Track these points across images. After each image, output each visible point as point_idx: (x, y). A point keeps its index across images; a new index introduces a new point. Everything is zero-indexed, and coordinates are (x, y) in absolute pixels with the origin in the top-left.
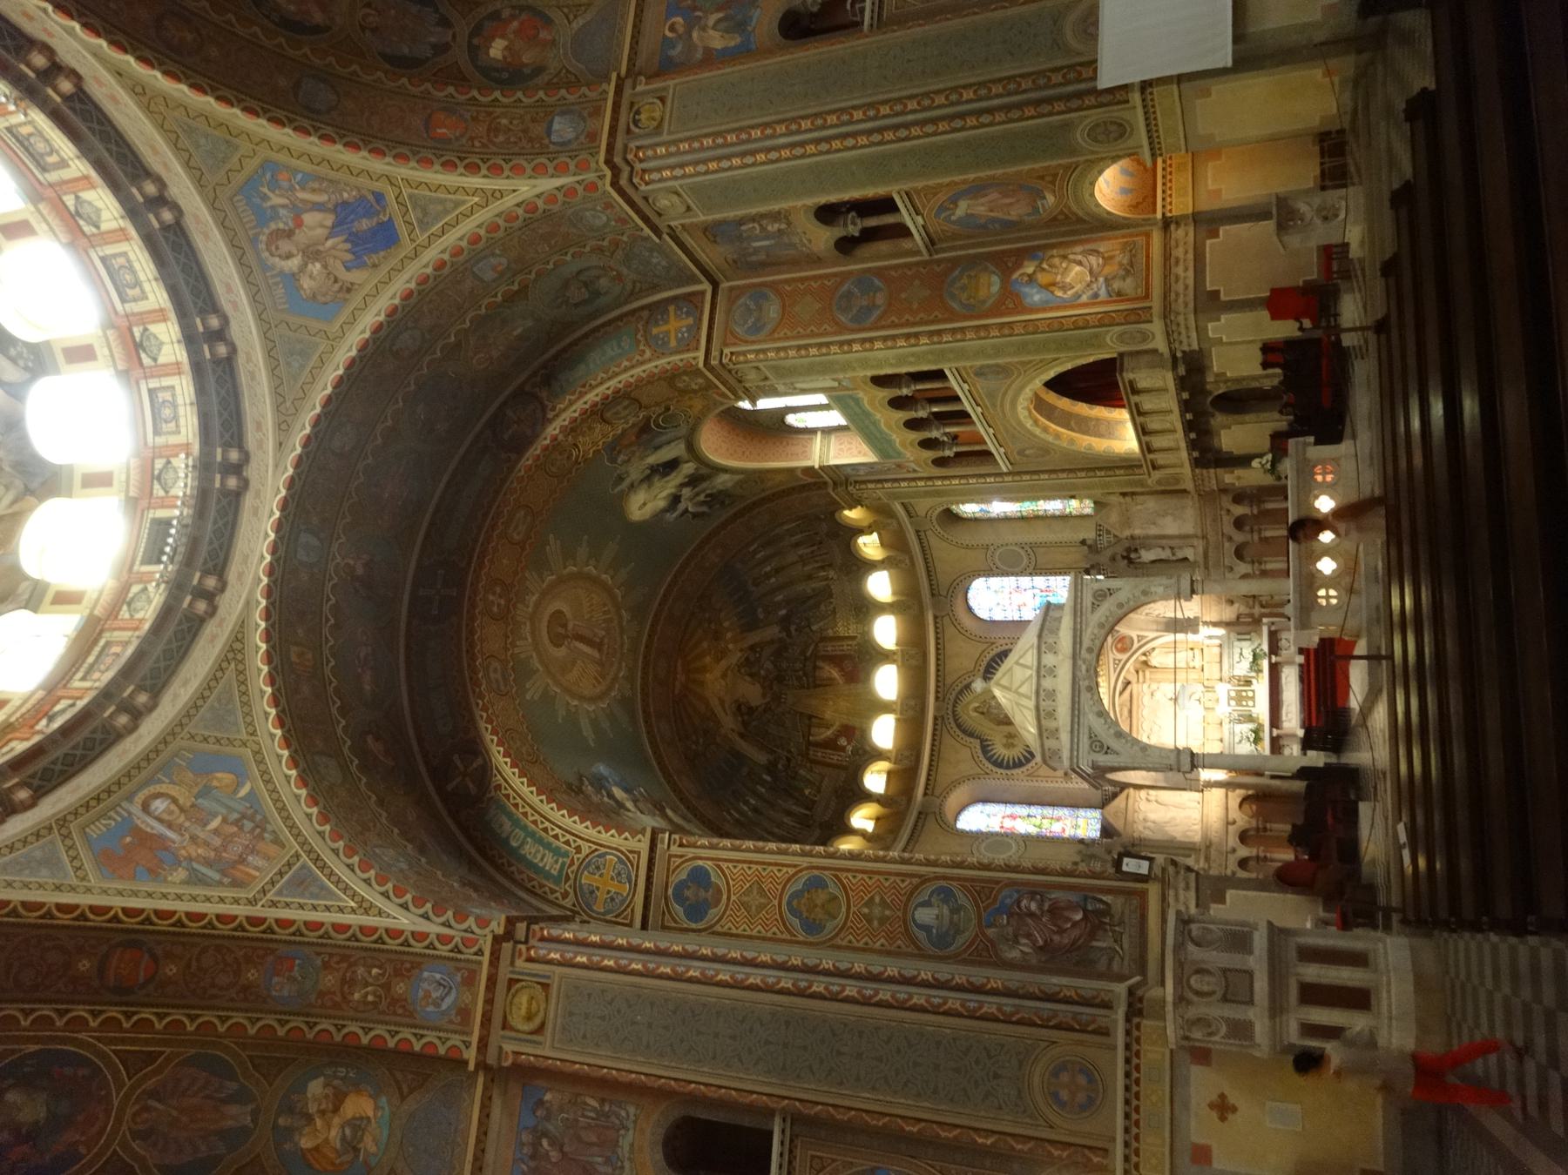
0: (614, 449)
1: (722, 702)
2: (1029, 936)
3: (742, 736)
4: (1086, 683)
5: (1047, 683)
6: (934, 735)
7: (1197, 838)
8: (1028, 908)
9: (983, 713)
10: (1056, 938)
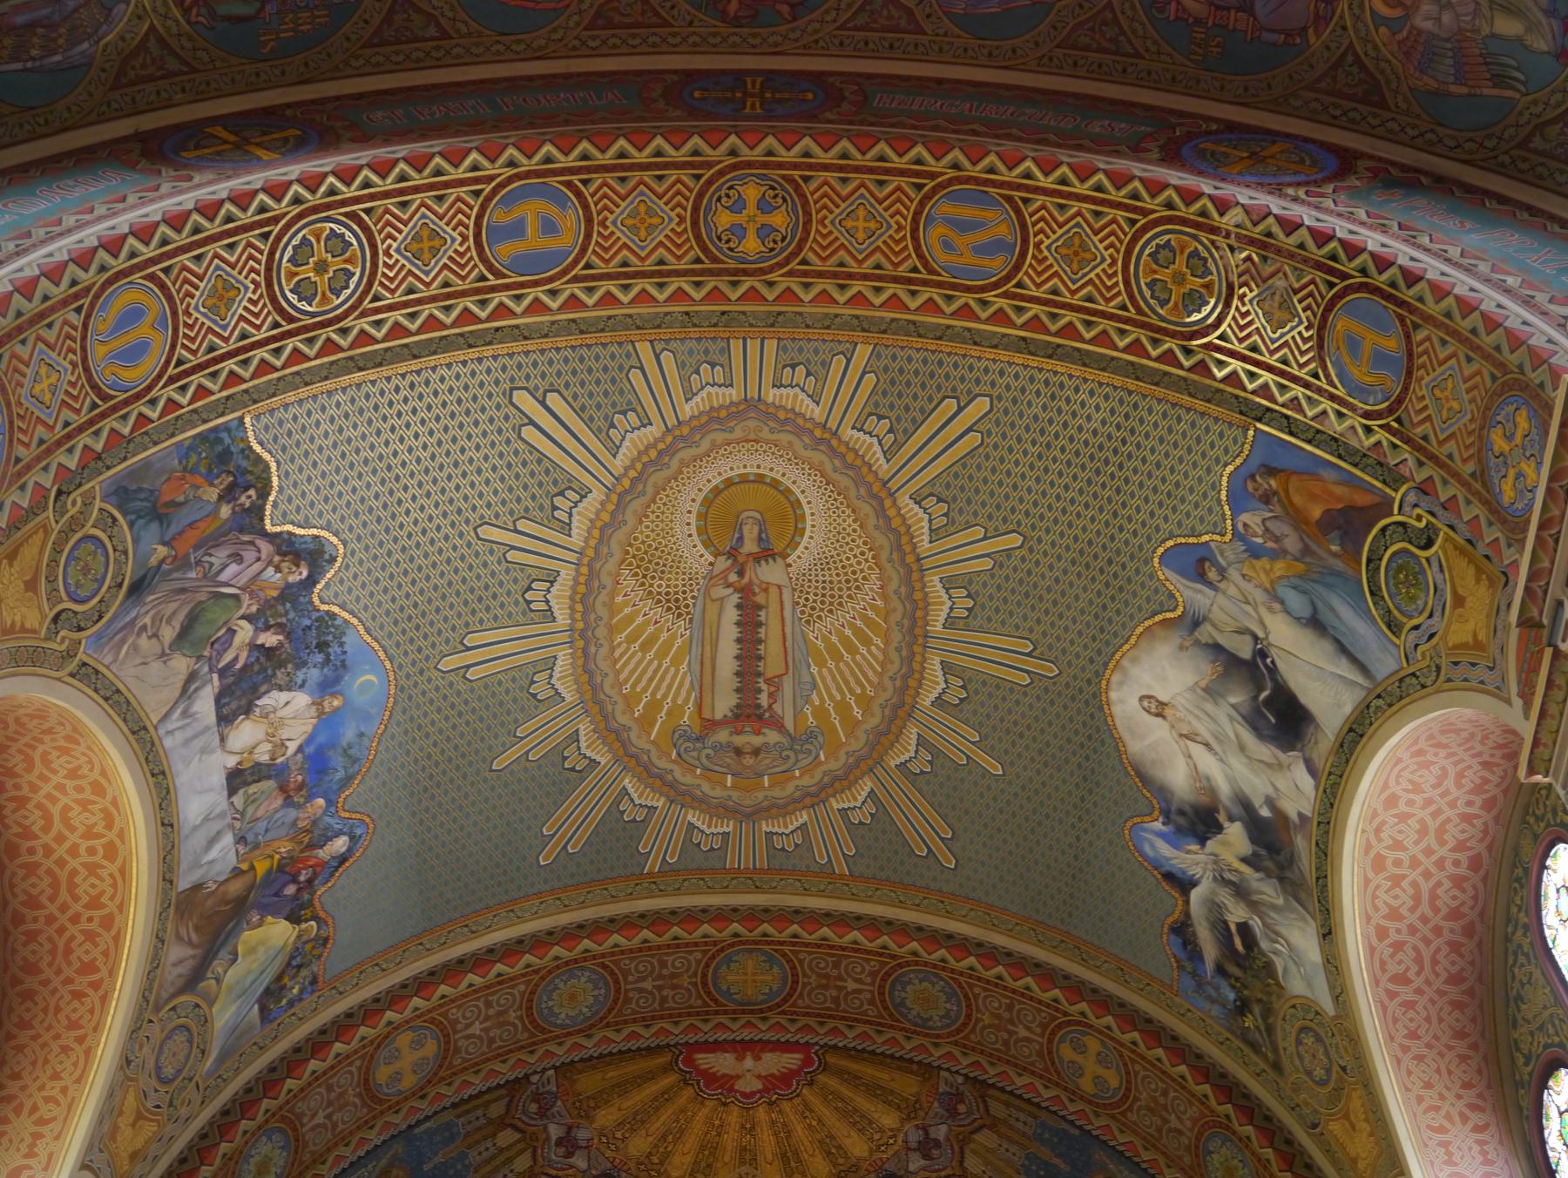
0: (1271, 471)
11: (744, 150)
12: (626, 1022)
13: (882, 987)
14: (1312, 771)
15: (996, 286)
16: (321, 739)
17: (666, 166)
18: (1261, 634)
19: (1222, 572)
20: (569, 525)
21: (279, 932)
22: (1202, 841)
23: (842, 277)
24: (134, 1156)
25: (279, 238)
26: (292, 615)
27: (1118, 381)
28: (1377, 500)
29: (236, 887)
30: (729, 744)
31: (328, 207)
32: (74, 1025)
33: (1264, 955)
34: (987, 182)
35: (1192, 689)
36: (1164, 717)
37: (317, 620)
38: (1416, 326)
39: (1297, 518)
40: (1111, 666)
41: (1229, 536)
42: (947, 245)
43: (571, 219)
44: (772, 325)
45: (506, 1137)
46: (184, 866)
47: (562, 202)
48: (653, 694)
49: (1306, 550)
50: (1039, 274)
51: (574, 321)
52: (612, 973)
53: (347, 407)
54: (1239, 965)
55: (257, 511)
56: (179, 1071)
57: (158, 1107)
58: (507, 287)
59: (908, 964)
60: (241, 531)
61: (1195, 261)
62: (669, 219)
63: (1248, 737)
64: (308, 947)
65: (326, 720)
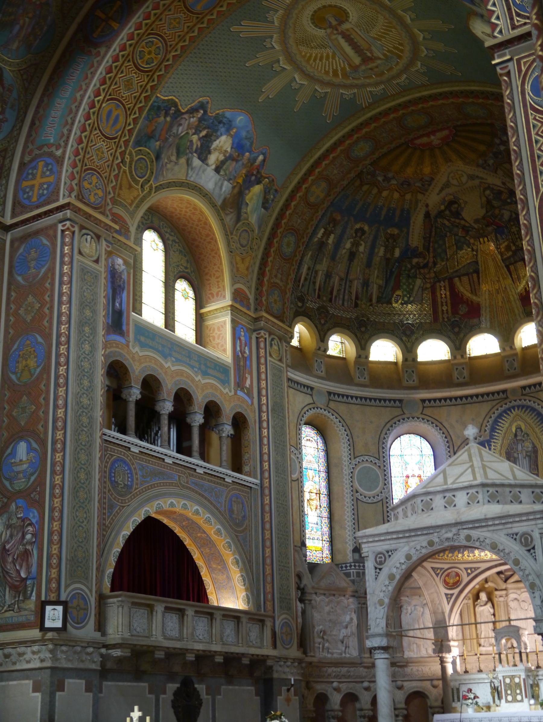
1: (447, 185)
2: (11, 536)
3: (427, 215)
4: (436, 540)
5: (438, 501)
6: (488, 394)
7: (408, 654)
8: (27, 533)
9: (516, 435)
10: (10, 559)
21: (257, 189)
24: (247, 269)
25: (133, 57)
26: (205, 123)
29: (236, 190)
32: (212, 250)
45: (365, 188)
48: (333, 68)
55: (177, 111)
60: (176, 118)
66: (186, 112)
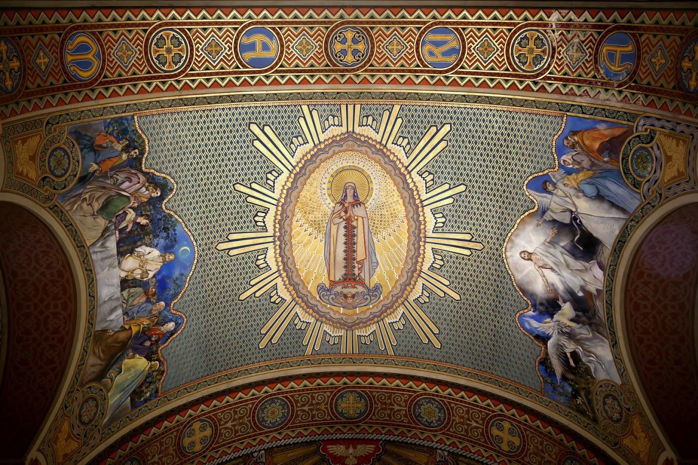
0: (575, 133)
11: (346, 16)
12: (296, 427)
13: (410, 408)
14: (601, 267)
15: (452, 69)
16: (164, 273)
17: (314, 23)
18: (574, 210)
19: (554, 185)
20: (274, 187)
21: (141, 363)
22: (552, 316)
23: (387, 71)
25: (151, 33)
27: (505, 108)
28: (625, 130)
29: (123, 336)
30: (342, 293)
31: (172, 24)
33: (584, 364)
34: (447, 23)
35: (543, 244)
36: (531, 260)
37: (164, 216)
38: (641, 35)
39: (587, 151)
40: (507, 240)
41: (557, 168)
42: (431, 54)
43: (274, 45)
44: (358, 98)
46: (99, 318)
47: (271, 37)
49: (593, 164)
50: (470, 61)
51: (276, 94)
52: (290, 402)
53: (179, 121)
54: (573, 373)
55: (138, 160)
56: (91, 421)
57: (79, 435)
58: (248, 72)
59: (421, 395)
61: (538, 41)
62: (316, 46)
63: (570, 260)
64: (155, 374)
65: (167, 266)
66: (145, 174)
